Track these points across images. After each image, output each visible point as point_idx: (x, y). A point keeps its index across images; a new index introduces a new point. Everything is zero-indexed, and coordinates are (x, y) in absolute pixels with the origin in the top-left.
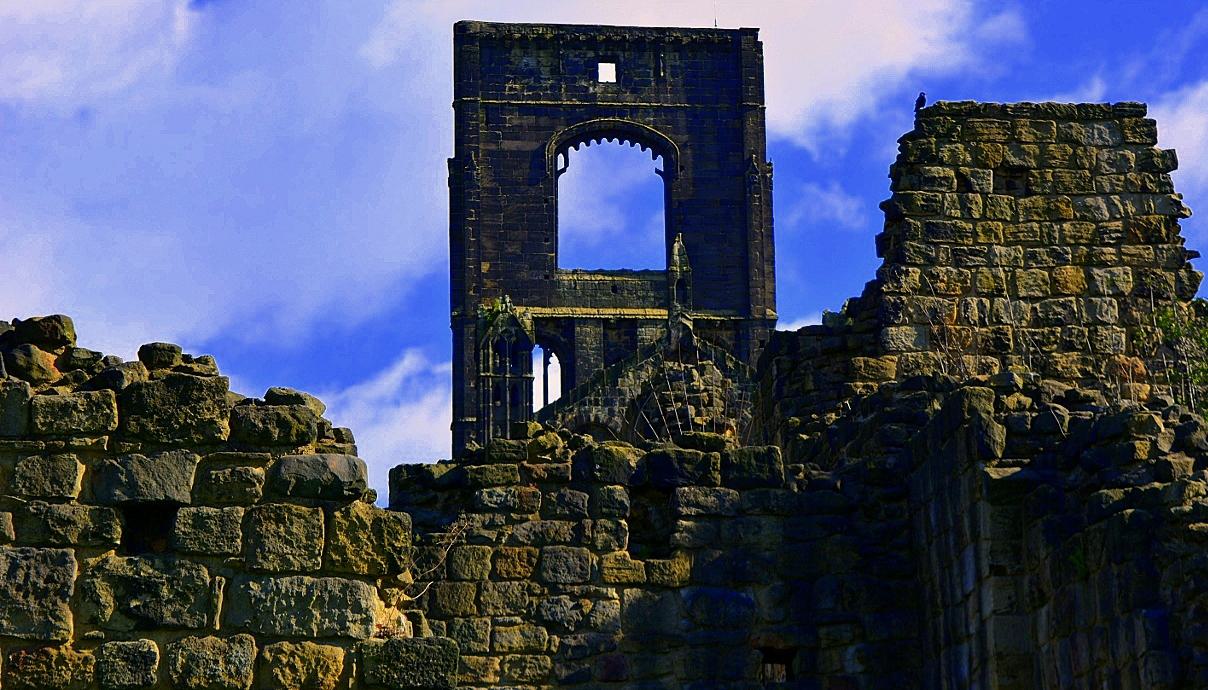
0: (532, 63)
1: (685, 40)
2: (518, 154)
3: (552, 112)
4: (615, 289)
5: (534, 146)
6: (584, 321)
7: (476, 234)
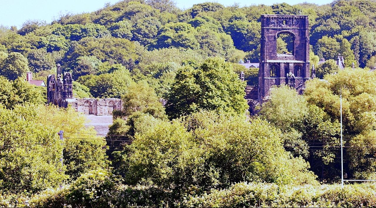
0: (274, 22)
1: (297, 17)
2: (271, 36)
3: (276, 29)
4: (285, 57)
5: (274, 35)
6: (281, 63)
7: (266, 49)
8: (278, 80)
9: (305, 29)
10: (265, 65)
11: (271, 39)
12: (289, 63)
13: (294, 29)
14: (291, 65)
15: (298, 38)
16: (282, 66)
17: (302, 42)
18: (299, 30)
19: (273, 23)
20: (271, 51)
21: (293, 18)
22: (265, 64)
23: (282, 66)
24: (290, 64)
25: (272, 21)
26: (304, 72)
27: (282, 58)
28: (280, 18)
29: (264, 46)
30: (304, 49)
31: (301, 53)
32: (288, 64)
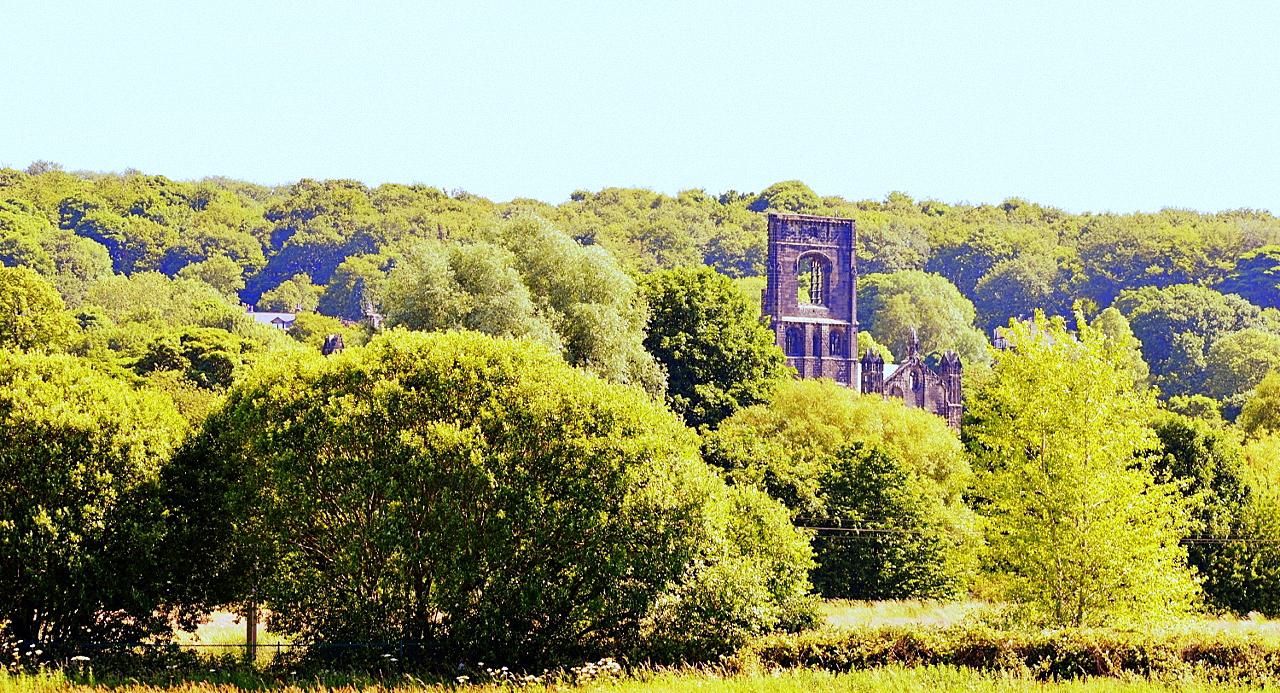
8: (800, 362)
9: (851, 250)
10: (778, 328)
11: (788, 270)
12: (820, 325)
13: (827, 248)
14: (826, 330)
15: (836, 269)
16: (810, 330)
17: (844, 279)
18: (838, 250)
19: (793, 233)
20: (787, 296)
21: (828, 224)
22: (779, 325)
23: (810, 330)
24: (826, 330)
25: (791, 229)
26: (847, 346)
27: (807, 314)
28: (806, 223)
29: (777, 285)
30: (846, 294)
31: (841, 303)
32: (819, 325)
